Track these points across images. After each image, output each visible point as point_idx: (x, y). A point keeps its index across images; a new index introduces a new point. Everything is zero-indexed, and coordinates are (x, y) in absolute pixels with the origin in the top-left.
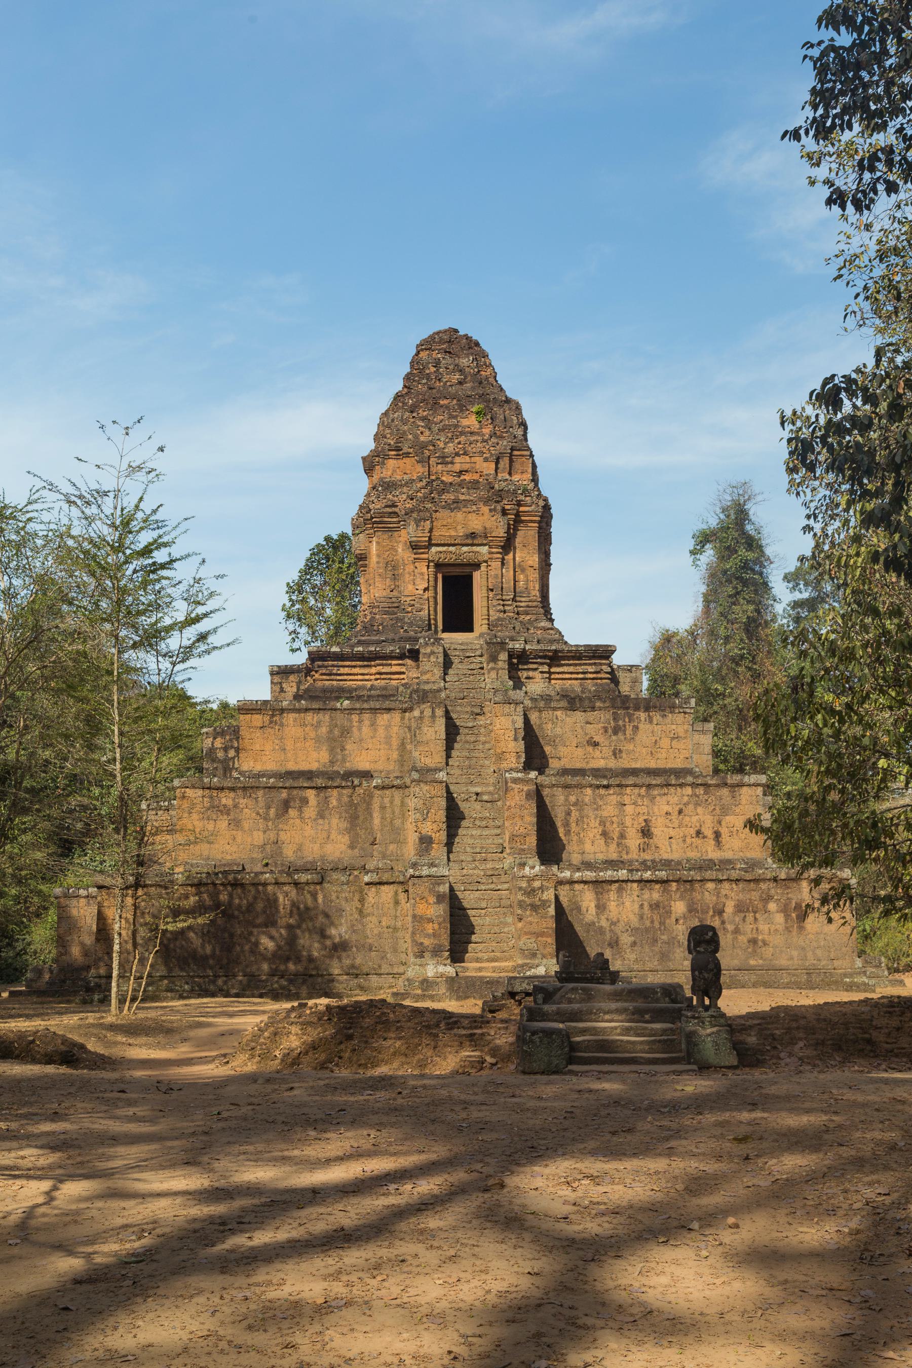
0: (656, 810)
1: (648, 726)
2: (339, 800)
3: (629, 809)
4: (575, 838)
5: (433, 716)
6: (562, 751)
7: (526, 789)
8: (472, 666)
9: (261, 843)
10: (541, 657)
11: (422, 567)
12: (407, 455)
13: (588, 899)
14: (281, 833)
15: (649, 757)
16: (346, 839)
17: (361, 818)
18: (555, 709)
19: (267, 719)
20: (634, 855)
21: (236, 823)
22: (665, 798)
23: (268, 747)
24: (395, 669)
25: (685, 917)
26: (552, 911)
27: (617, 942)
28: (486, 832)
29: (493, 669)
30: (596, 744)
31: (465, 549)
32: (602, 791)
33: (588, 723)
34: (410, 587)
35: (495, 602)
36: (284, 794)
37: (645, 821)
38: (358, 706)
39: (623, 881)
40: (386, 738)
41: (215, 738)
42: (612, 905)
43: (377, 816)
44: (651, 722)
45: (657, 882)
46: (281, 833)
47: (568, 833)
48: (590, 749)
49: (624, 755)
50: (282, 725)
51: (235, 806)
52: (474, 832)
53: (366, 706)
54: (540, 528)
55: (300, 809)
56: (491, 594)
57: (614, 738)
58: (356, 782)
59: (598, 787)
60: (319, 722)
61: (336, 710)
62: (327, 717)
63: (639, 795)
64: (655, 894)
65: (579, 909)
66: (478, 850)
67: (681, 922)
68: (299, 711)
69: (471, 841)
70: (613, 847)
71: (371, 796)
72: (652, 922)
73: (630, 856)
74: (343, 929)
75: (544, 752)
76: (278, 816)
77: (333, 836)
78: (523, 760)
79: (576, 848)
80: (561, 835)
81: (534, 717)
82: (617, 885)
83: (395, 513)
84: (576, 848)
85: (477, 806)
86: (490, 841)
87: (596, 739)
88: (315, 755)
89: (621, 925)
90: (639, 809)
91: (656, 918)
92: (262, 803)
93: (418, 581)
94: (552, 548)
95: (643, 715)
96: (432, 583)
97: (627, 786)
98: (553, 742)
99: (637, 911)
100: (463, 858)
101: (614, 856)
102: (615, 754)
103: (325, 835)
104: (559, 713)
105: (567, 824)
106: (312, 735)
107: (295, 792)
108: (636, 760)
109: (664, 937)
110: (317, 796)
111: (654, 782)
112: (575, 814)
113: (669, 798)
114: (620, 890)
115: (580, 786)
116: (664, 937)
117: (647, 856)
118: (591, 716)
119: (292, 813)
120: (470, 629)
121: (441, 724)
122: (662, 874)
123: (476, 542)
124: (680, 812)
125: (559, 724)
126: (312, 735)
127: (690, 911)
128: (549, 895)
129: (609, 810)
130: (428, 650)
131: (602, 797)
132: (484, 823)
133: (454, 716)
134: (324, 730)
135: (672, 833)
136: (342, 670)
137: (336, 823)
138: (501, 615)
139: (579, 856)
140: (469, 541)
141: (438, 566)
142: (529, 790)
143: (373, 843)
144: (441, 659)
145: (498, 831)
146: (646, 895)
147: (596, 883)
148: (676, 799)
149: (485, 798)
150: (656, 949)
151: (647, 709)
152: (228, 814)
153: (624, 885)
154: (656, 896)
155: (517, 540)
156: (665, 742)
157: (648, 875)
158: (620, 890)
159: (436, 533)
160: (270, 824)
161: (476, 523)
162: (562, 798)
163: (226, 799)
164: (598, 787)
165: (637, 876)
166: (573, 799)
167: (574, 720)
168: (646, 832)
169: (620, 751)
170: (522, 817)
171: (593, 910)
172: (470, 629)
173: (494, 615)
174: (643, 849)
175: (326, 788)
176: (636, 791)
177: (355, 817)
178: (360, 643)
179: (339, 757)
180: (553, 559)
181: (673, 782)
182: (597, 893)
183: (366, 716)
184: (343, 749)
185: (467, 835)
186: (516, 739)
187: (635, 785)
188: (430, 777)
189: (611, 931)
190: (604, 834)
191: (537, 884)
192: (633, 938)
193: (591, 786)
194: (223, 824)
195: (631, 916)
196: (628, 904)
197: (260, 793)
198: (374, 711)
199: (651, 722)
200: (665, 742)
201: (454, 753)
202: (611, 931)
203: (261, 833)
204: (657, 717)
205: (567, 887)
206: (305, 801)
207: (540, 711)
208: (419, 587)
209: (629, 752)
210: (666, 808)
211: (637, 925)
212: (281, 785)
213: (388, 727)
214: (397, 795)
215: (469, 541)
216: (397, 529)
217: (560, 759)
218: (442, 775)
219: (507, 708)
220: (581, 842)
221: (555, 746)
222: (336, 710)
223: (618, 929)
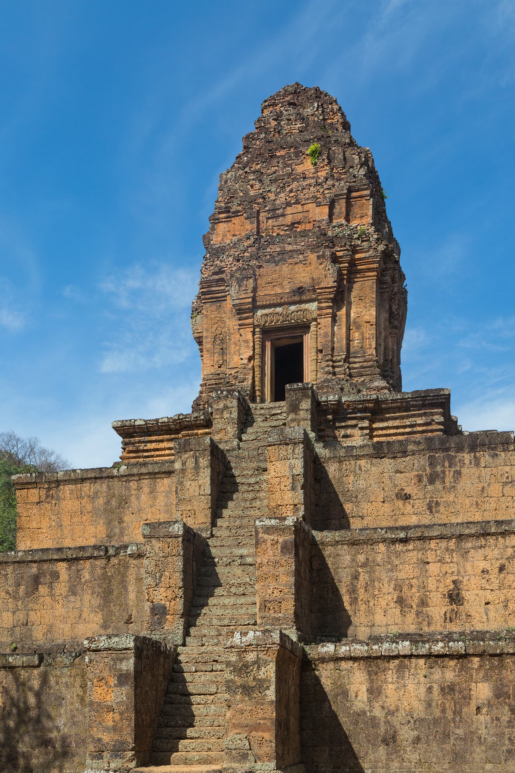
0: (469, 567)
1: (474, 470)
2: (92, 573)
3: (433, 568)
4: (363, 607)
5: (197, 467)
6: (366, 508)
7: (281, 540)
8: (275, 423)
9: (10, 625)
10: (361, 411)
13: (358, 681)
14: (31, 613)
15: (473, 509)
16: (98, 618)
17: (115, 593)
18: (357, 458)
19: (43, 492)
20: (438, 627)
22: (481, 551)
23: (45, 524)
25: (490, 705)
27: (394, 738)
28: (242, 600)
29: (293, 420)
30: (407, 497)
32: (399, 547)
33: (398, 472)
36: (34, 569)
37: (454, 582)
38: (135, 471)
39: (405, 656)
40: (166, 505)
42: (390, 689)
43: (130, 589)
44: (477, 464)
45: (451, 656)
46: (31, 613)
47: (354, 601)
48: (400, 503)
49: (442, 509)
50: (58, 499)
52: (227, 601)
53: (144, 470)
55: (51, 586)
57: (430, 488)
58: (111, 552)
59: (394, 541)
60: (96, 493)
61: (113, 477)
62: (104, 486)
63: (447, 549)
64: (450, 673)
65: (345, 694)
66: (226, 622)
67: (484, 710)
69: (220, 612)
70: (411, 617)
71: (127, 567)
72: (444, 711)
73: (432, 628)
74: (61, 722)
75: (343, 510)
76: (28, 594)
77: (85, 615)
79: (363, 619)
80: (347, 605)
82: (397, 662)
83: (222, 280)
84: (363, 619)
85: (238, 571)
86: (243, 611)
87: (408, 490)
88: (92, 529)
89: (401, 716)
90: (446, 568)
91: (449, 705)
92: (11, 581)
95: (467, 457)
97: (431, 538)
98: (354, 498)
99: (423, 696)
100: (205, 632)
101: (412, 629)
102: (430, 508)
103: (77, 615)
104: (362, 462)
105: (353, 591)
106: (89, 507)
107: (45, 566)
108: (456, 514)
109: (460, 732)
110: (69, 569)
111: (467, 531)
112: (363, 577)
113: (487, 551)
114: (401, 668)
115: (371, 542)
116: (460, 732)
117: (455, 628)
118: (402, 462)
119: (43, 590)
121: (205, 478)
122: (459, 646)
124: (502, 569)
125: (363, 475)
126: (89, 507)
127: (497, 696)
129: (407, 571)
130: (221, 405)
131: (398, 555)
133: (236, 472)
134: (101, 501)
135: (490, 597)
137: (89, 600)
139: (368, 630)
142: (285, 542)
143: (128, 622)
146: (437, 674)
147: (368, 659)
148: (496, 552)
150: (448, 747)
151: (473, 449)
153: (406, 661)
154: (450, 675)
155: (353, 294)
156: (495, 489)
157: (439, 648)
158: (401, 668)
159: (260, 293)
160: (20, 603)
161: (303, 275)
162: (348, 558)
164: (394, 541)
165: (424, 650)
166: (361, 558)
167: (380, 469)
168: (455, 597)
169: (437, 504)
170: (276, 578)
171: (363, 695)
174: (449, 618)
175: (77, 559)
176: (443, 544)
177: (109, 593)
179: (117, 531)
181: (493, 530)
182: (369, 673)
183: (146, 482)
184: (121, 521)
185: (219, 606)
186: (293, 489)
187: (442, 537)
188: (163, 531)
189: (387, 722)
190: (400, 601)
192: (416, 733)
193: (384, 541)
195: (416, 704)
196: (411, 687)
197: (10, 569)
198: (153, 475)
199: (477, 465)
200: (495, 489)
201: (226, 513)
202: (387, 722)
203: (10, 614)
204: (485, 458)
205: (331, 665)
206: (56, 576)
207: (340, 462)
208: (243, 352)
209: (448, 505)
210: (483, 565)
211: (422, 715)
212: (30, 558)
217: (362, 518)
219: (284, 451)
220: (370, 612)
221: (357, 503)
222: (113, 477)
223: (396, 721)
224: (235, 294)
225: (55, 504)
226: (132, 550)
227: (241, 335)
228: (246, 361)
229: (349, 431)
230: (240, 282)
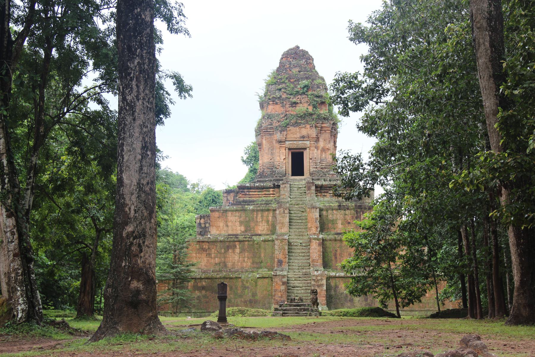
8: (301, 192)
12: (277, 103)
19: (221, 214)
21: (209, 255)
24: (271, 192)
26: (325, 288)
28: (304, 258)
31: (300, 142)
34: (278, 158)
35: (312, 164)
41: (201, 219)
50: (226, 216)
51: (209, 248)
54: (331, 132)
56: (311, 161)
68: (233, 211)
78: (319, 230)
81: (324, 213)
88: (239, 228)
93: (281, 156)
94: (338, 140)
96: (287, 156)
119: (230, 251)
120: (302, 174)
128: (324, 282)
132: (303, 255)
136: (251, 193)
138: (315, 169)
140: (302, 139)
141: (289, 149)
144: (289, 190)
145: (308, 258)
149: (304, 245)
159: (288, 136)
161: (304, 132)
163: (206, 246)
172: (302, 174)
173: (312, 170)
178: (258, 181)
180: (337, 145)
186: (316, 222)
191: (319, 278)
194: (204, 255)
213: (268, 216)
214: (270, 243)
215: (302, 139)
216: (273, 134)
218: (286, 237)
224: (278, 136)
229: (325, 194)
230: (281, 132)
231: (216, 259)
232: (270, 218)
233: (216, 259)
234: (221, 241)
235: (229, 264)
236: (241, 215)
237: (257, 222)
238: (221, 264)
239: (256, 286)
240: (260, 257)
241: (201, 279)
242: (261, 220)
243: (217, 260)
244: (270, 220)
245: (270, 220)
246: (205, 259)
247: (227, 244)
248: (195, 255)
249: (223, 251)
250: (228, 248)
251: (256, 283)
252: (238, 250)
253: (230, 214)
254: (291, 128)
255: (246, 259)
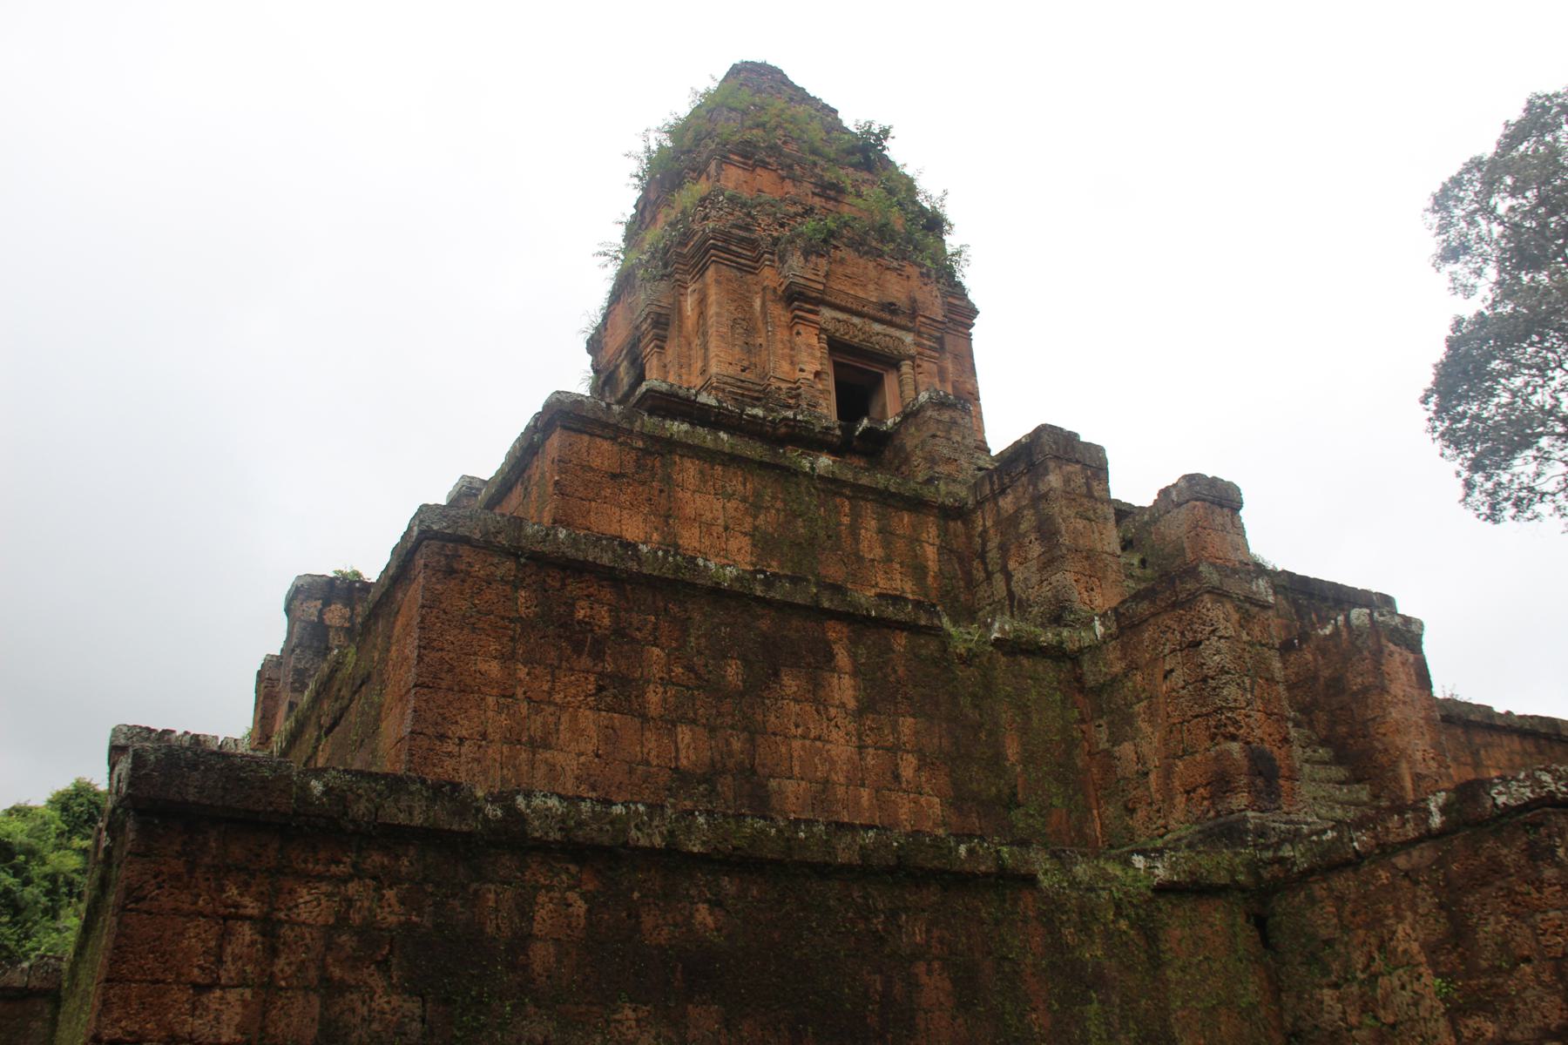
11: (809, 338)
21: (619, 692)
31: (877, 327)
51: (619, 632)
93: (804, 356)
119: (791, 683)
123: (897, 320)
152: (598, 655)
225: (661, 491)
226: (1002, 629)
227: (798, 333)
228: (811, 377)
231: (684, 734)
232: (931, 552)
233: (684, 734)
234: (716, 593)
235: (791, 793)
236: (758, 494)
237: (860, 559)
238: (726, 785)
239: (1156, 963)
240: (996, 760)
241: (671, 859)
242: (878, 552)
243: (690, 746)
244: (933, 566)
245: (933, 566)
246: (587, 718)
247: (764, 625)
248: (494, 668)
249: (733, 672)
250: (769, 662)
251: (1151, 936)
252: (844, 689)
253: (689, 471)
254: (845, 253)
255: (907, 771)
